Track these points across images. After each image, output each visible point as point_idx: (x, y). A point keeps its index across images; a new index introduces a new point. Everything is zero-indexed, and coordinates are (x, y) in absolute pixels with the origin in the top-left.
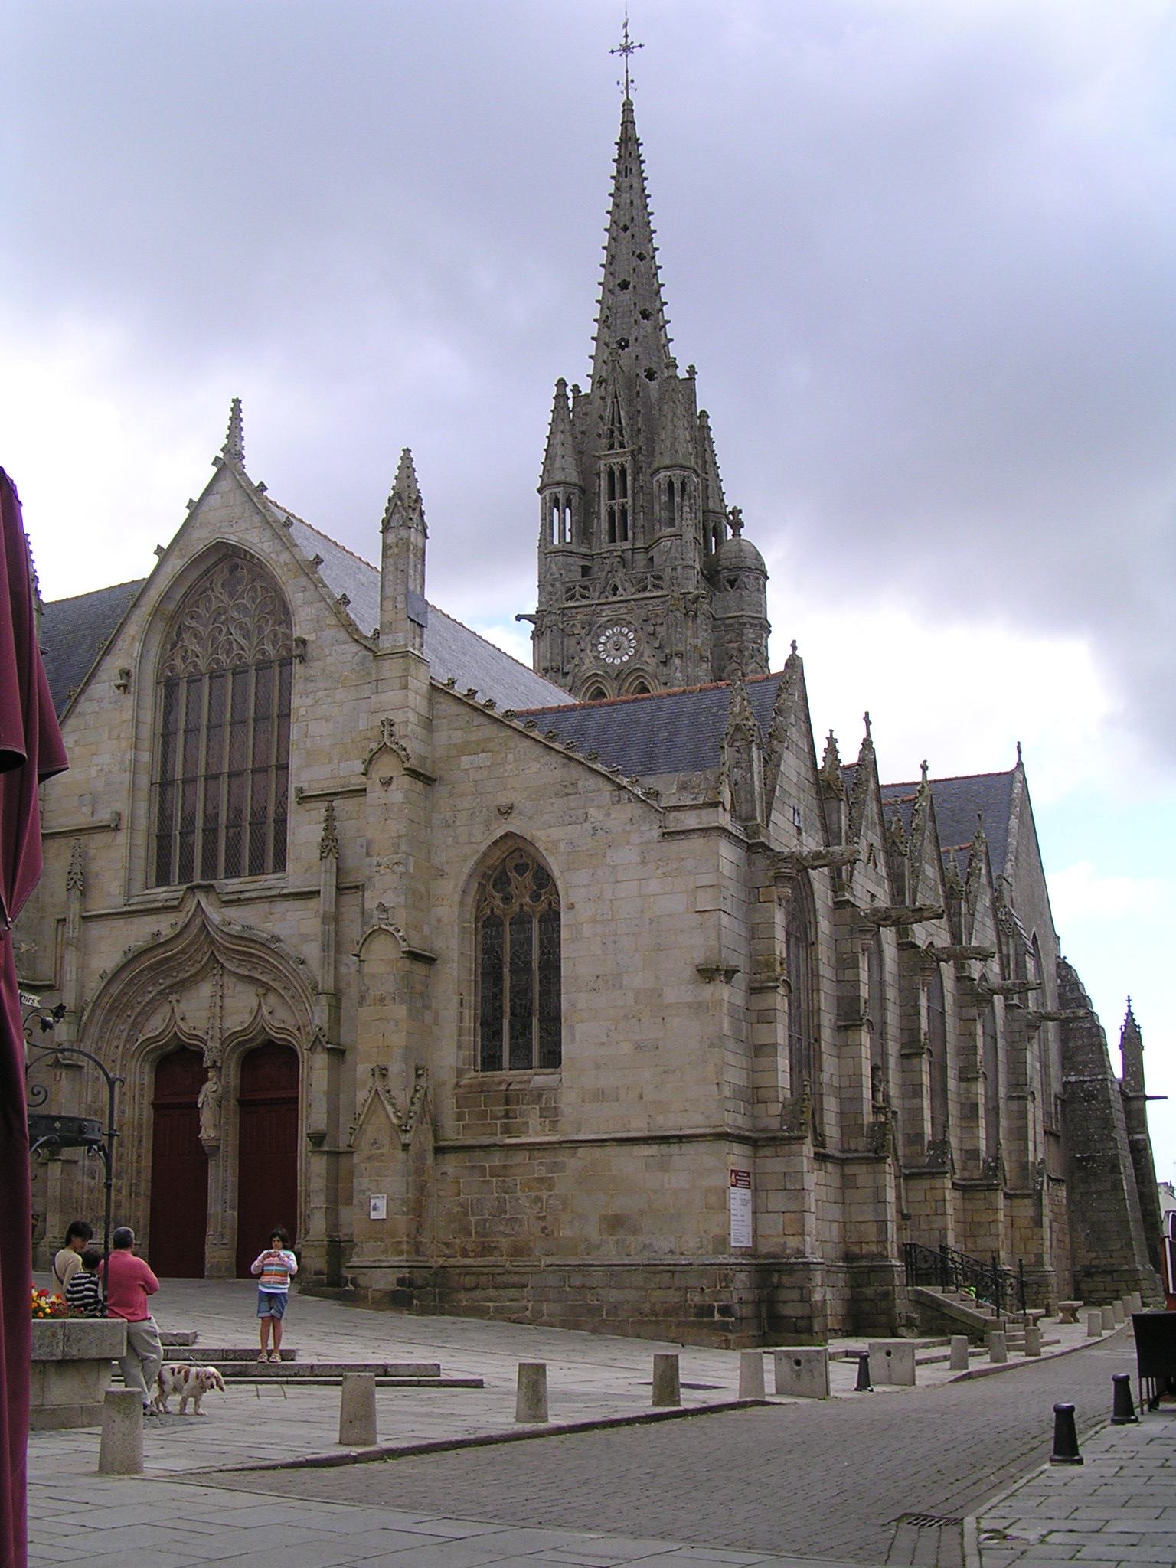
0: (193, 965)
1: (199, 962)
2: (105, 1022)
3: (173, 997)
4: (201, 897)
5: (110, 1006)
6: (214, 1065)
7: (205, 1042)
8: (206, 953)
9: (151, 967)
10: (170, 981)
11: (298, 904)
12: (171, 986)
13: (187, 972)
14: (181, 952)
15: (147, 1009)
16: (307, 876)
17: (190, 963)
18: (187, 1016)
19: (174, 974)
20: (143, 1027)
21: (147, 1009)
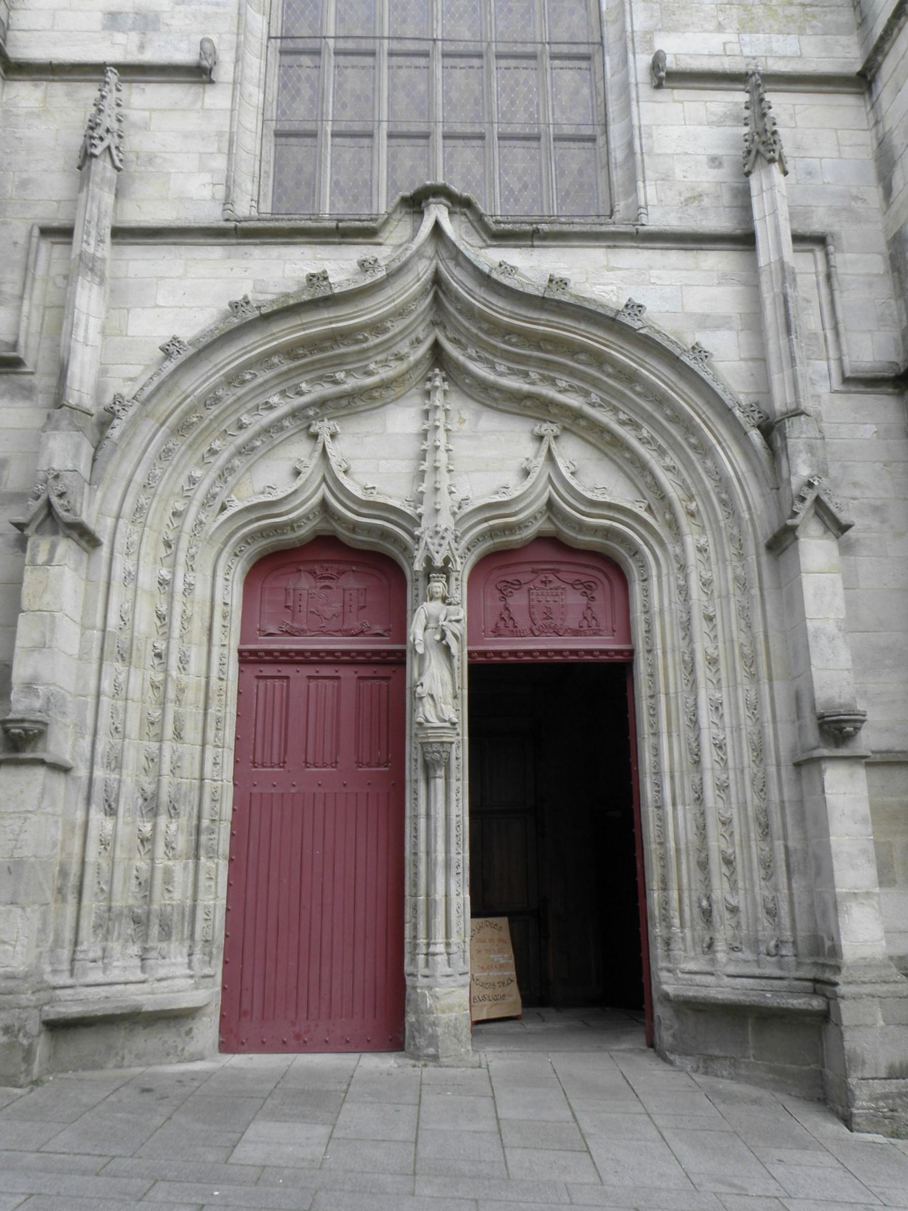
0: (385, 363)
1: (400, 358)
2: (165, 454)
3: (323, 427)
4: (437, 212)
5: (181, 418)
6: (430, 569)
7: (416, 521)
8: (418, 341)
9: (290, 351)
10: (328, 390)
11: (675, 258)
12: (322, 403)
13: (369, 374)
14: (376, 327)
15: (258, 443)
16: (691, 210)
17: (378, 358)
18: (355, 466)
19: (340, 376)
20: (237, 484)
21: (258, 443)
